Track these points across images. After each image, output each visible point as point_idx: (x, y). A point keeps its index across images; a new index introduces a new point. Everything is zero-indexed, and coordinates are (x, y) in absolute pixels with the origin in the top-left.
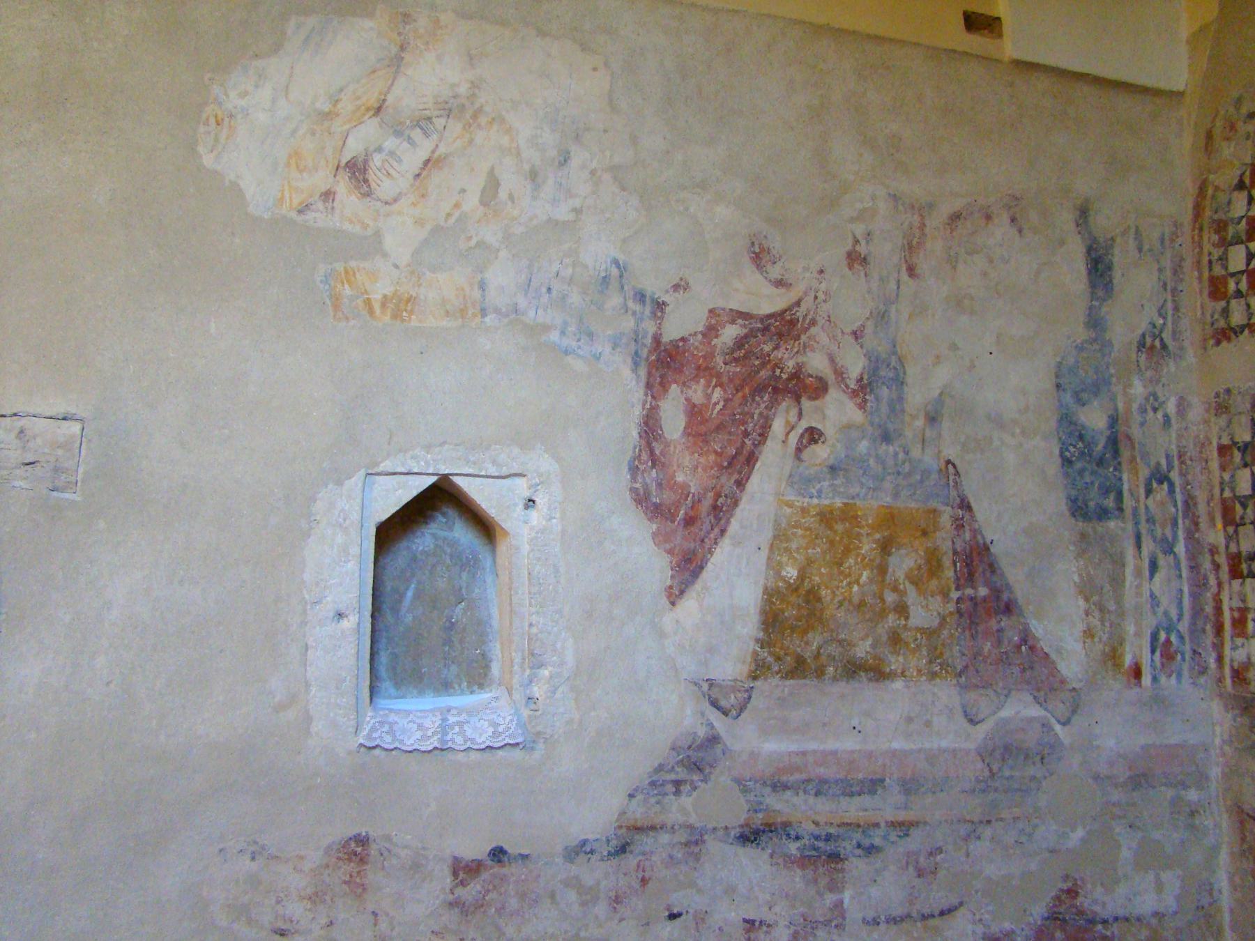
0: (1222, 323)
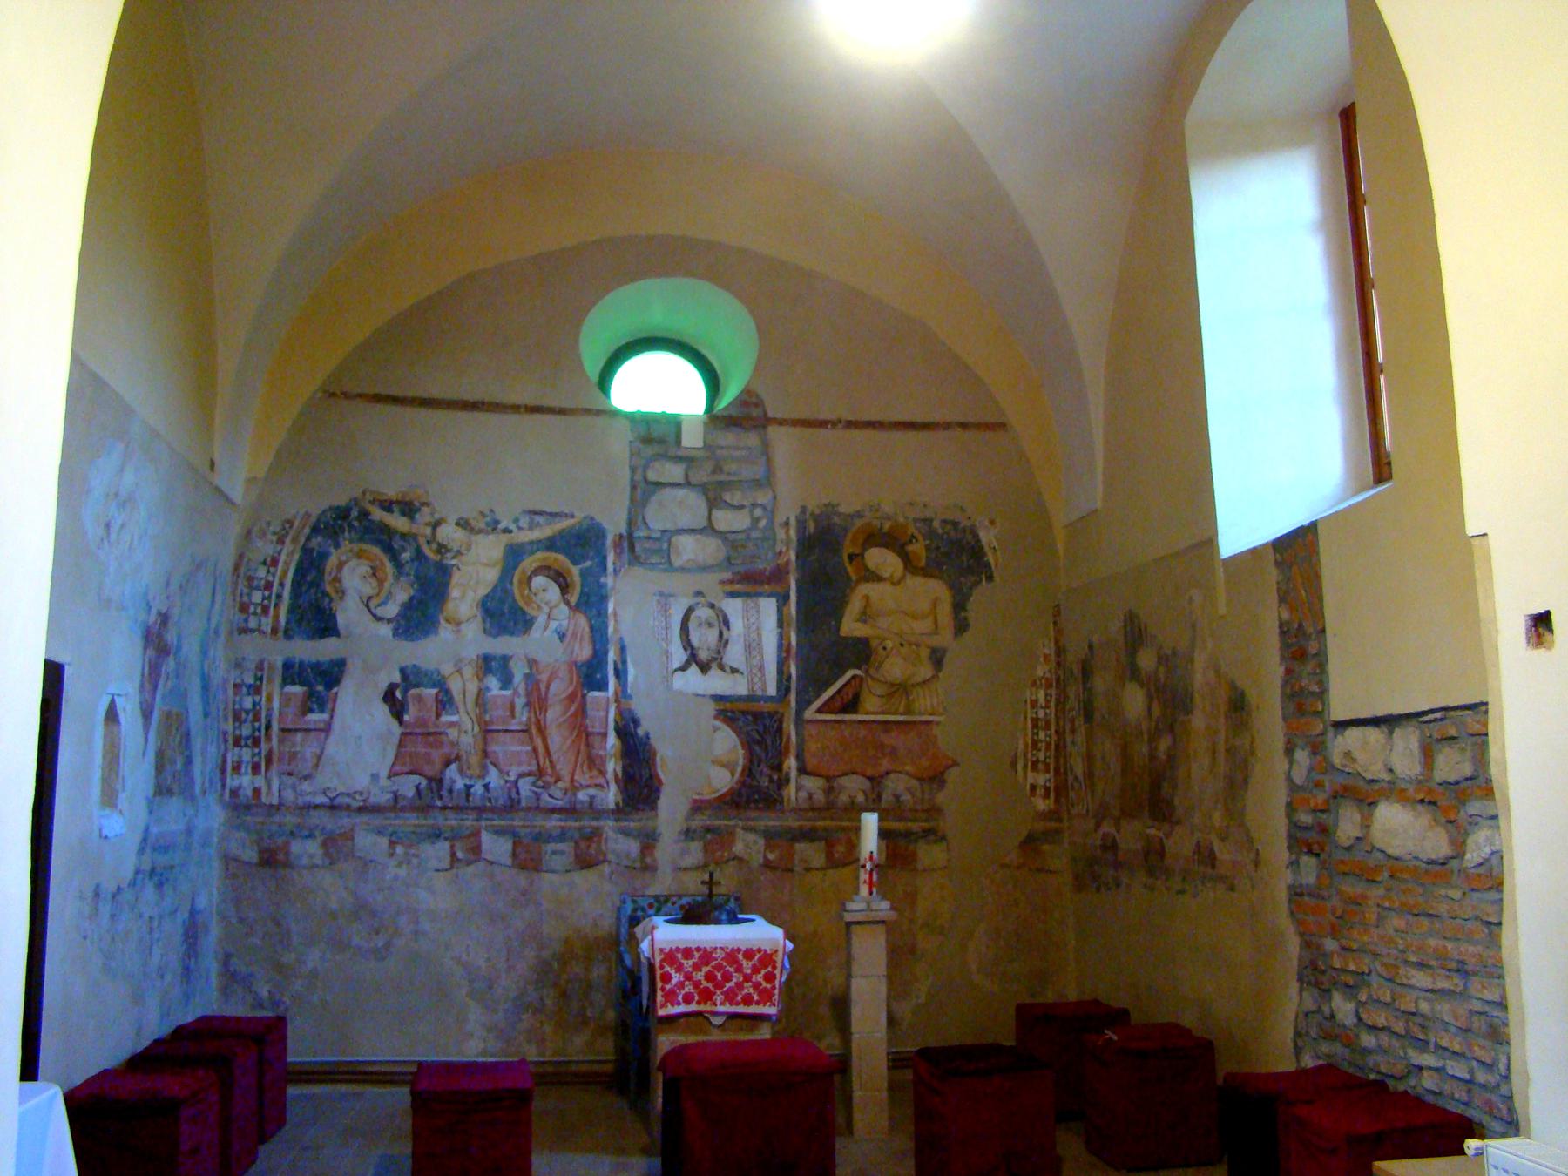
0: (242, 625)
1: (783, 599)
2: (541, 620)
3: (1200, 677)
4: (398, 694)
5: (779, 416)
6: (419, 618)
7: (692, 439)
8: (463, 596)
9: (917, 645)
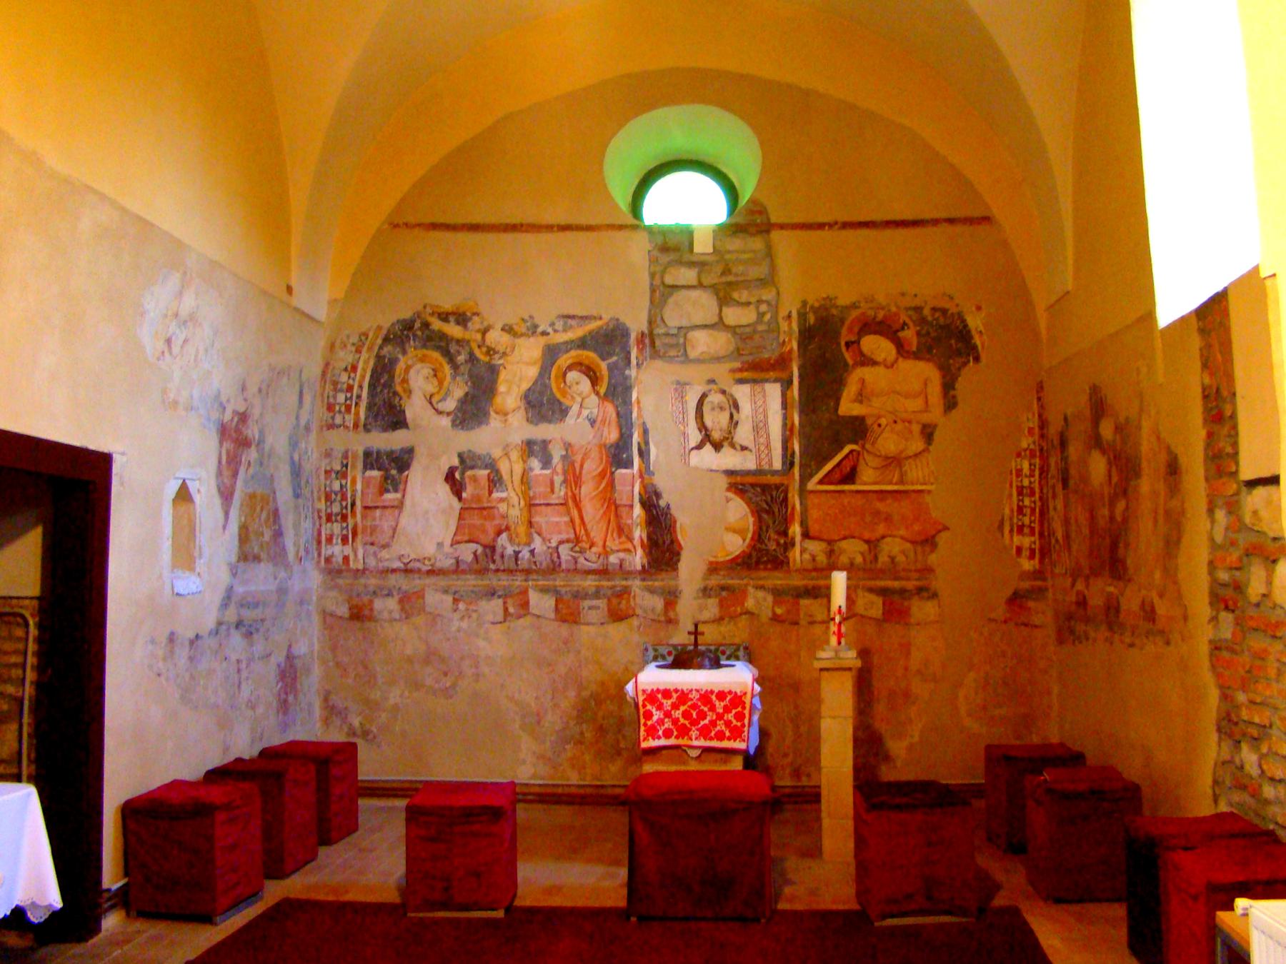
1: (787, 384)
2: (575, 408)
3: (1146, 445)
4: (457, 476)
5: (780, 221)
6: (473, 410)
7: (703, 246)
8: (508, 392)
9: (910, 422)
